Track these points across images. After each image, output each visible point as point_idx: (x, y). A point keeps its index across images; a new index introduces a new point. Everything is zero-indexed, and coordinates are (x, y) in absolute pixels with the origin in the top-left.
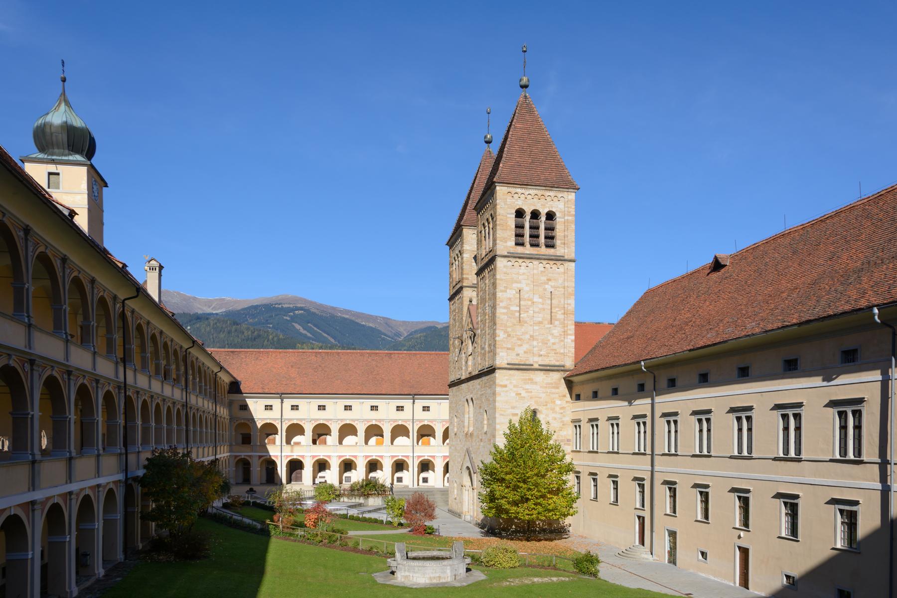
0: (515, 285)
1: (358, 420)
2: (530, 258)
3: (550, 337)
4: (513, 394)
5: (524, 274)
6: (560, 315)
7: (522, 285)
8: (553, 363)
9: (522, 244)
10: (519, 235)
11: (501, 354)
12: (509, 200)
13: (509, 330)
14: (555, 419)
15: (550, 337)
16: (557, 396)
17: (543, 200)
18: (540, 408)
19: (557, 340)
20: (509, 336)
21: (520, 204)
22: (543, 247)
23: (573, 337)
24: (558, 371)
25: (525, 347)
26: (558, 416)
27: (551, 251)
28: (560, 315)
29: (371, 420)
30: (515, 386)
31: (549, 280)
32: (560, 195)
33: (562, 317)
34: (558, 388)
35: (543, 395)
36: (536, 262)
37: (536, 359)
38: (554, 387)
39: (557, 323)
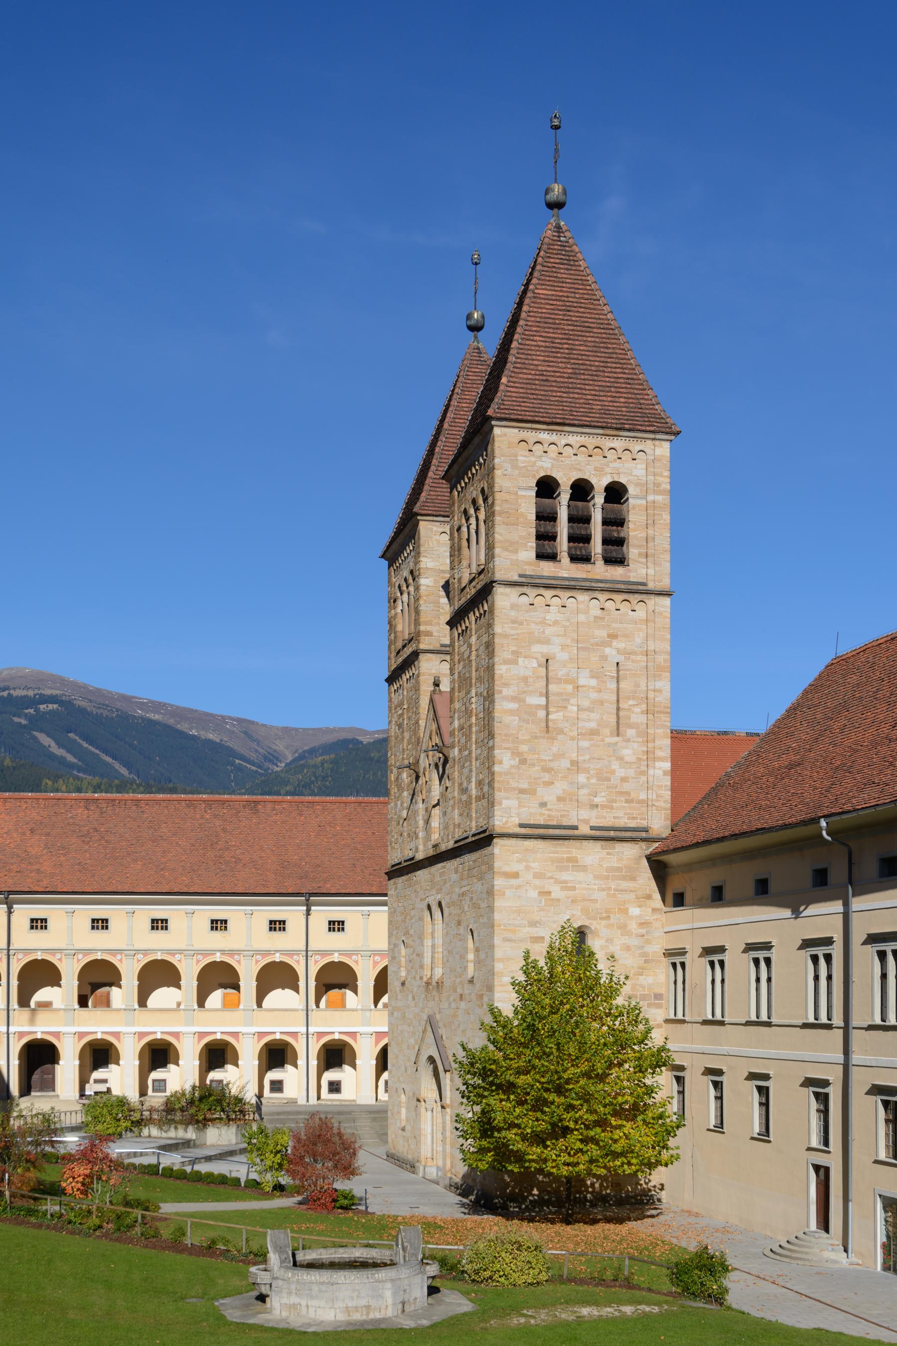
0: (537, 649)
1: (181, 951)
2: (571, 586)
4: (533, 894)
5: (556, 623)
6: (637, 716)
8: (624, 822)
9: (552, 557)
10: (545, 537)
12: (523, 458)
13: (524, 748)
14: (628, 948)
15: (615, 766)
16: (632, 896)
17: (597, 460)
18: (593, 925)
19: (631, 772)
20: (523, 761)
21: (546, 466)
22: (600, 563)
23: (667, 765)
24: (633, 840)
25: (560, 787)
26: (634, 942)
27: (616, 573)
28: (637, 716)
29: (212, 952)
30: (537, 876)
31: (612, 636)
32: (636, 446)
33: (643, 719)
34: (633, 879)
35: (600, 896)
36: (583, 597)
37: (585, 814)
38: (624, 878)
39: (631, 733)
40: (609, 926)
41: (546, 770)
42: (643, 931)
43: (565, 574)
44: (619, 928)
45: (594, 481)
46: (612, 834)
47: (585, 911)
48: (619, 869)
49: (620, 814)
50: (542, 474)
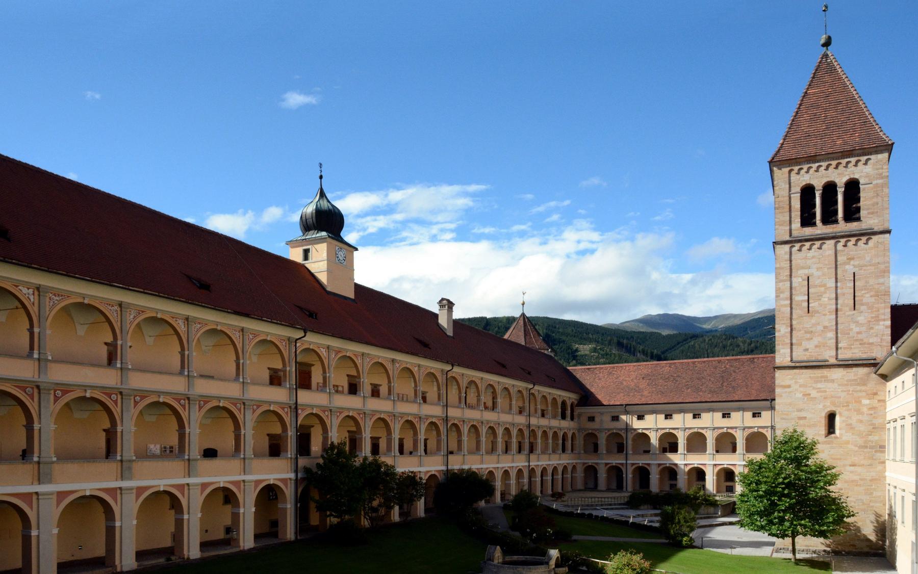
0: (801, 272)
2: (823, 238)
5: (813, 257)
7: (813, 272)
14: (861, 421)
25: (816, 340)
32: (864, 158)
34: (864, 385)
35: (843, 395)
38: (858, 384)
40: (849, 410)
43: (819, 232)
44: (855, 410)
45: (837, 181)
46: (850, 362)
47: (833, 403)
48: (855, 380)
50: (804, 183)
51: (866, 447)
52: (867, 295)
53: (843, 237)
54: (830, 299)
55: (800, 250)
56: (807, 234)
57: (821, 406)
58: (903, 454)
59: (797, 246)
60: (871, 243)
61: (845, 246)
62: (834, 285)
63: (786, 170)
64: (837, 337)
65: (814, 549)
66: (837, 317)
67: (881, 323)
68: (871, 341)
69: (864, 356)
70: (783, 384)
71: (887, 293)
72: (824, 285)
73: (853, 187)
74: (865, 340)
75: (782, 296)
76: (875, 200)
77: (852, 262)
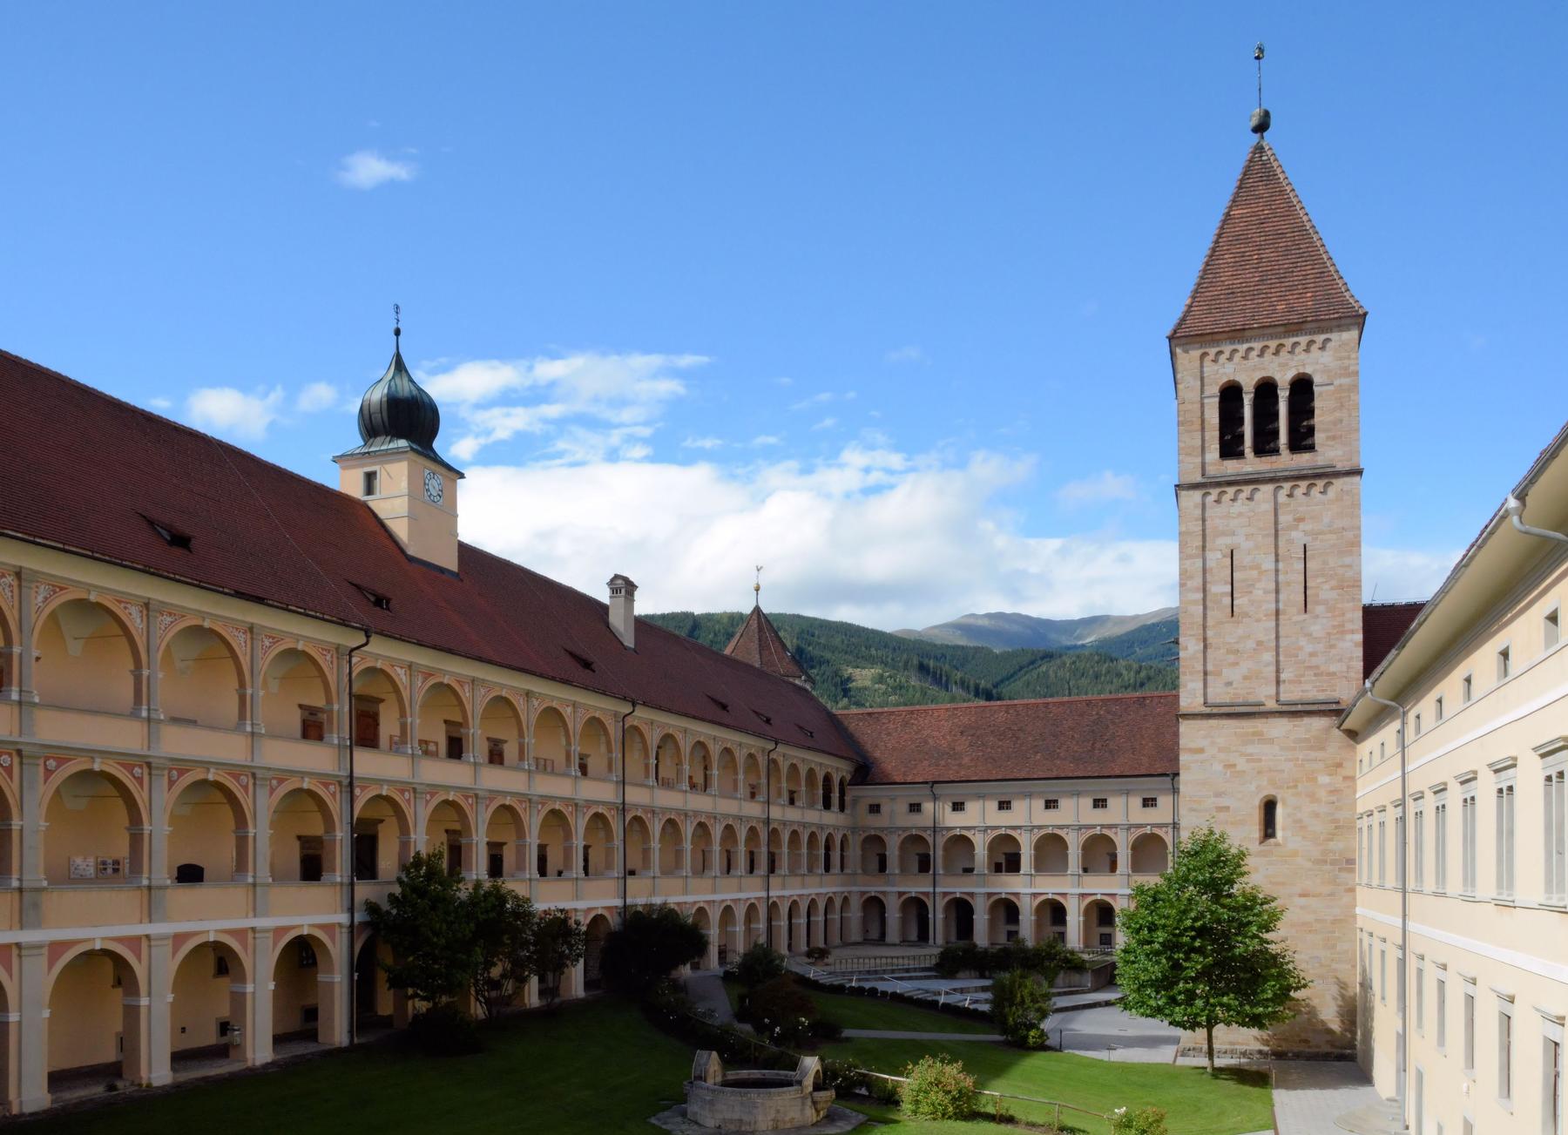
2: (1255, 480)
3: (1303, 642)
5: (1240, 514)
7: (1240, 541)
11: (1191, 685)
14: (1317, 815)
25: (1245, 667)
32: (1320, 338)
34: (1323, 749)
36: (1268, 489)
38: (1312, 748)
41: (1229, 652)
42: (1334, 798)
43: (1248, 469)
46: (1300, 708)
48: (1307, 740)
49: (1308, 687)
50: (1225, 380)
51: (1325, 862)
52: (1326, 586)
53: (1286, 479)
54: (1266, 592)
55: (1218, 501)
56: (1230, 471)
57: (1253, 787)
58: (1382, 876)
59: (1215, 492)
60: (1332, 491)
61: (1290, 496)
62: (1272, 566)
63: (1196, 353)
64: (1278, 662)
65: (1244, 1048)
66: (1277, 625)
67: (1349, 637)
68: (1332, 668)
69: (1322, 697)
70: (1192, 745)
71: (1356, 584)
72: (1257, 567)
73: (1303, 388)
74: (1323, 668)
75: (1189, 584)
76: (1337, 414)
77: (1302, 526)
